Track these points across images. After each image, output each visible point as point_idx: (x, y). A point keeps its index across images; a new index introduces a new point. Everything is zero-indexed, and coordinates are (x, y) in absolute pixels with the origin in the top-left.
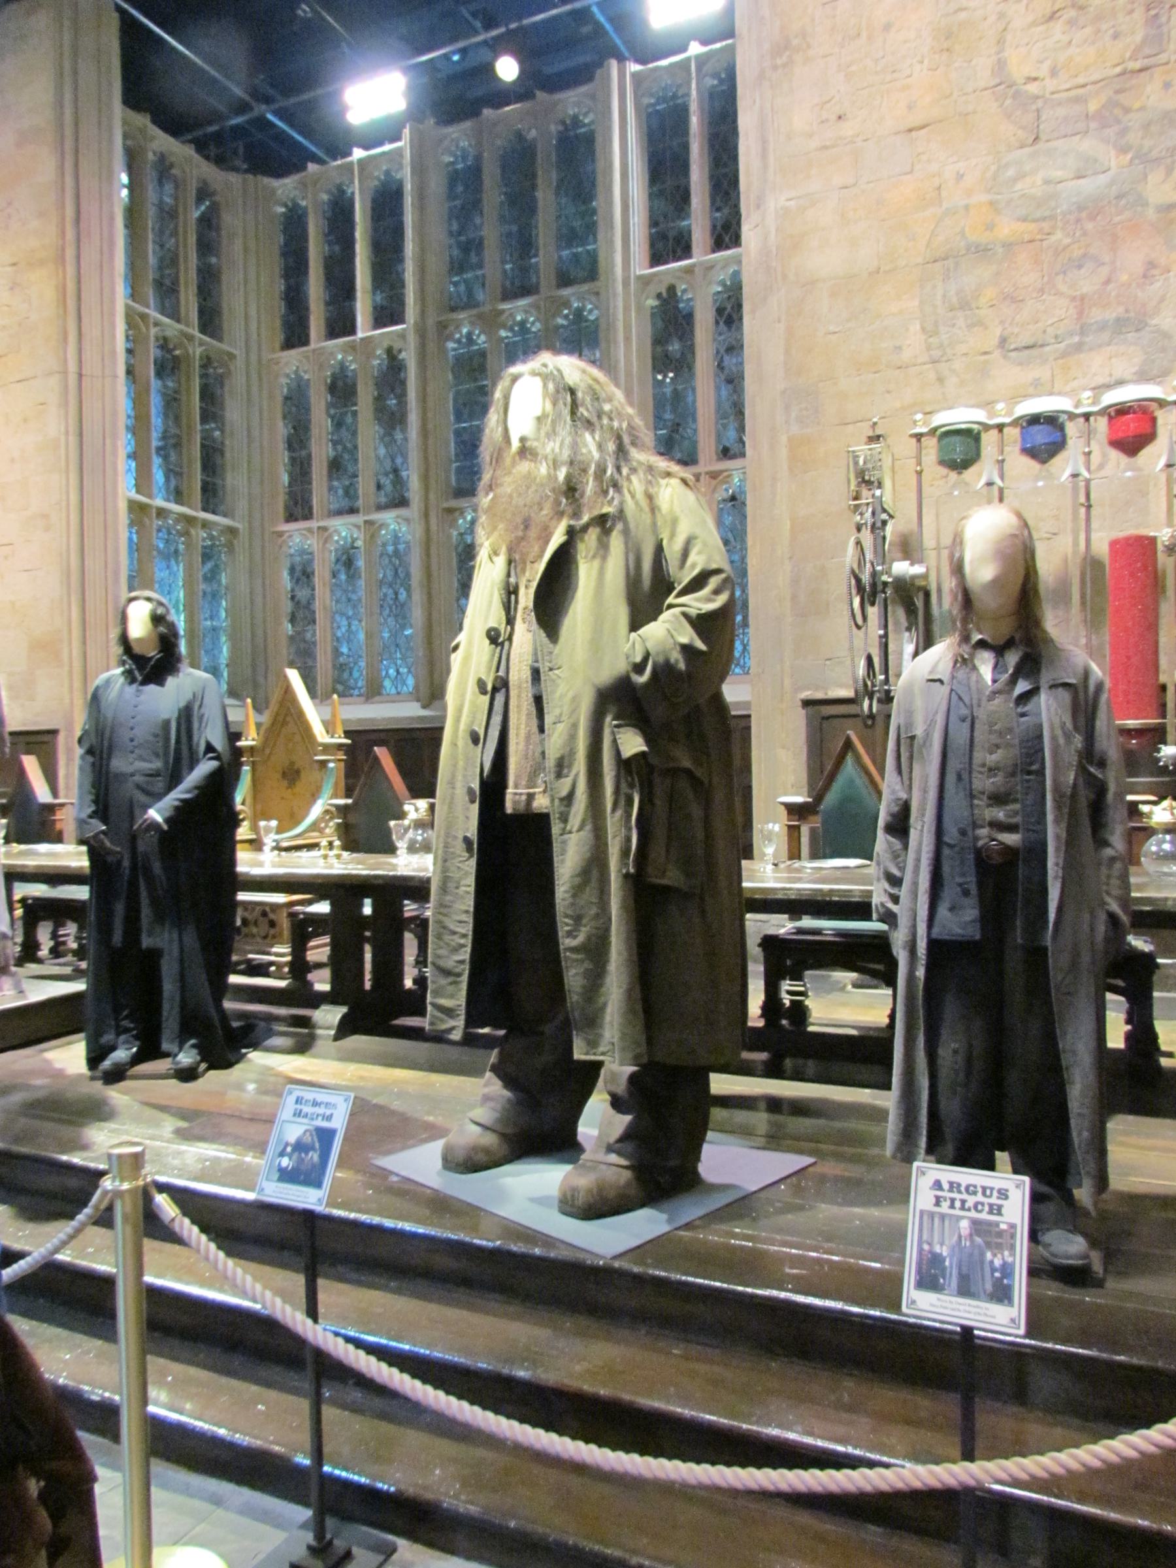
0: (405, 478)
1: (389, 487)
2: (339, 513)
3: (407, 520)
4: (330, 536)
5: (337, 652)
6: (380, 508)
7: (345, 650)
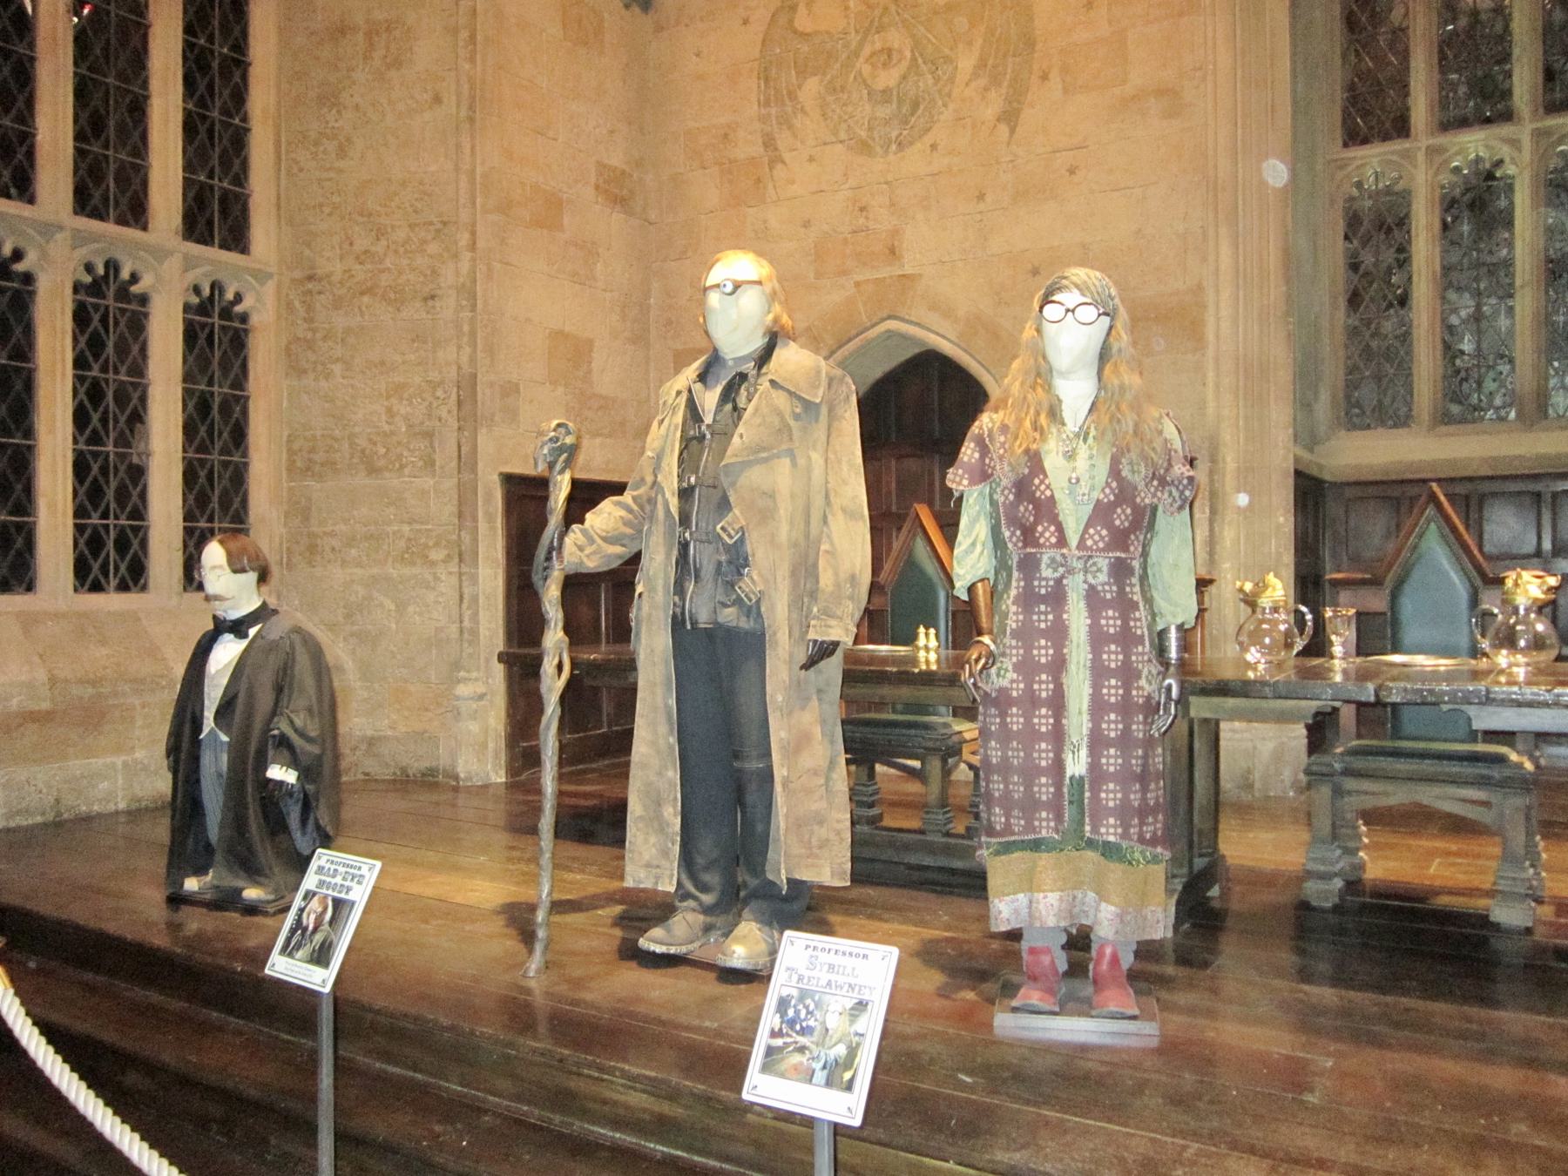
5: (1450, 352)
7: (1467, 345)
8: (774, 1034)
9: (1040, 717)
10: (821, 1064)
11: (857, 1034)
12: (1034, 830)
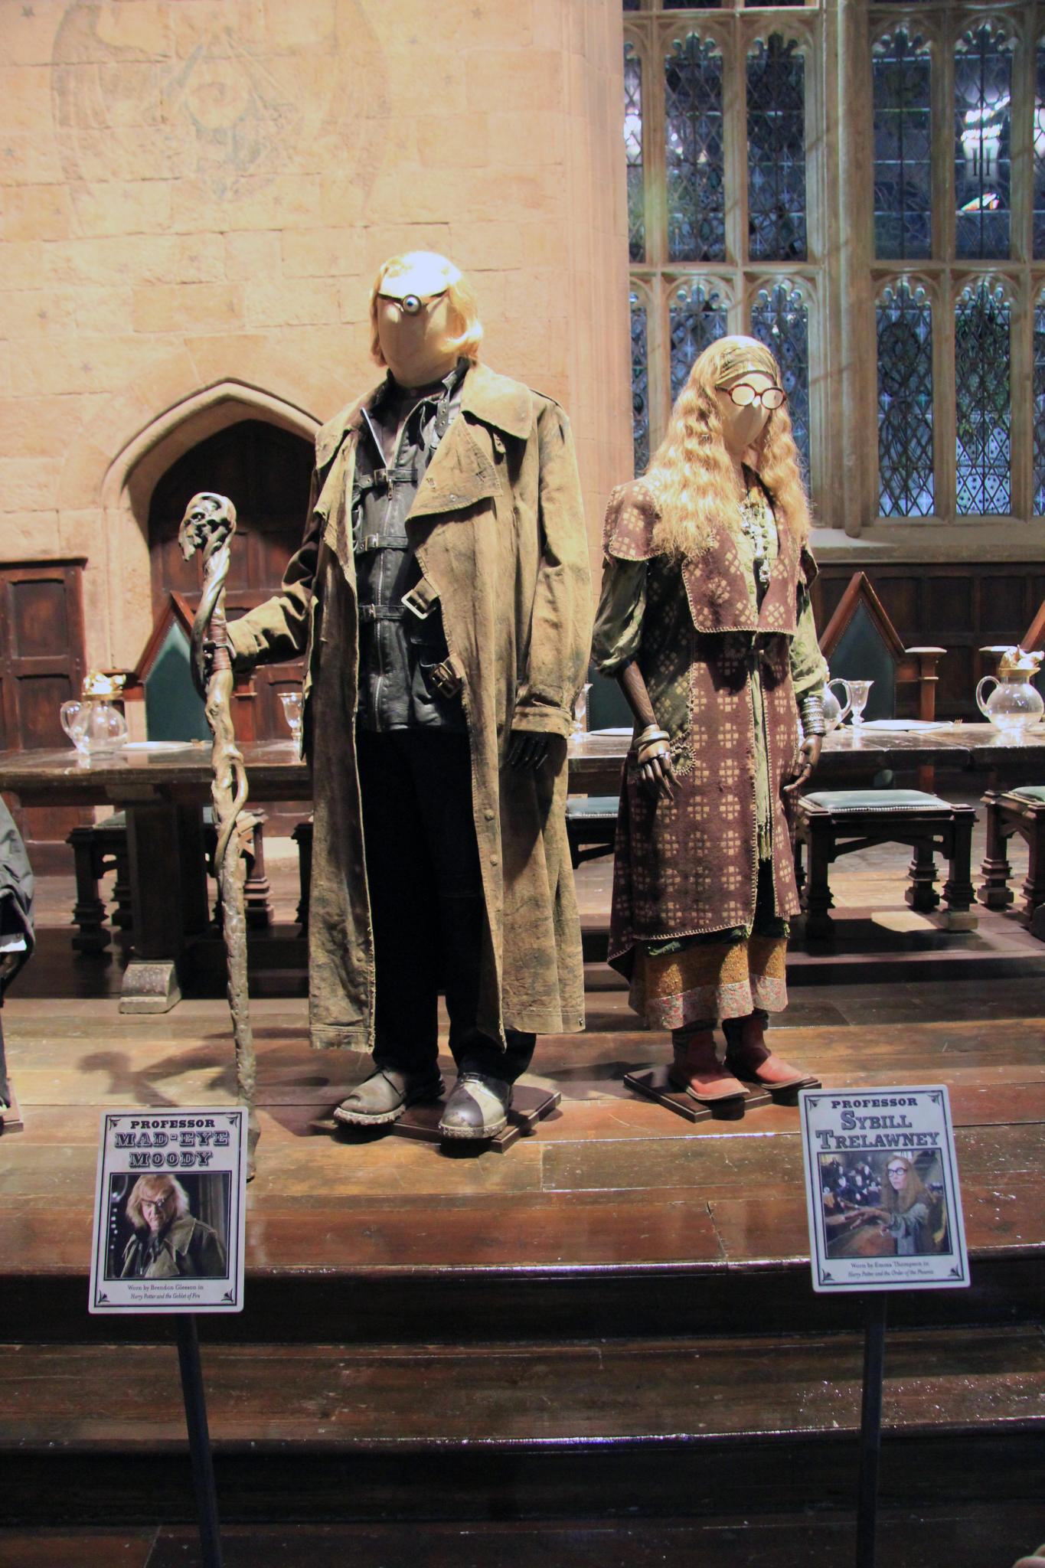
0: (796, 223)
1: (771, 233)
2: (687, 258)
3: (811, 280)
4: (678, 288)
6: (753, 257)
8: (828, 1211)
9: (726, 804)
10: (902, 1232)
11: (933, 1188)
12: (722, 921)
